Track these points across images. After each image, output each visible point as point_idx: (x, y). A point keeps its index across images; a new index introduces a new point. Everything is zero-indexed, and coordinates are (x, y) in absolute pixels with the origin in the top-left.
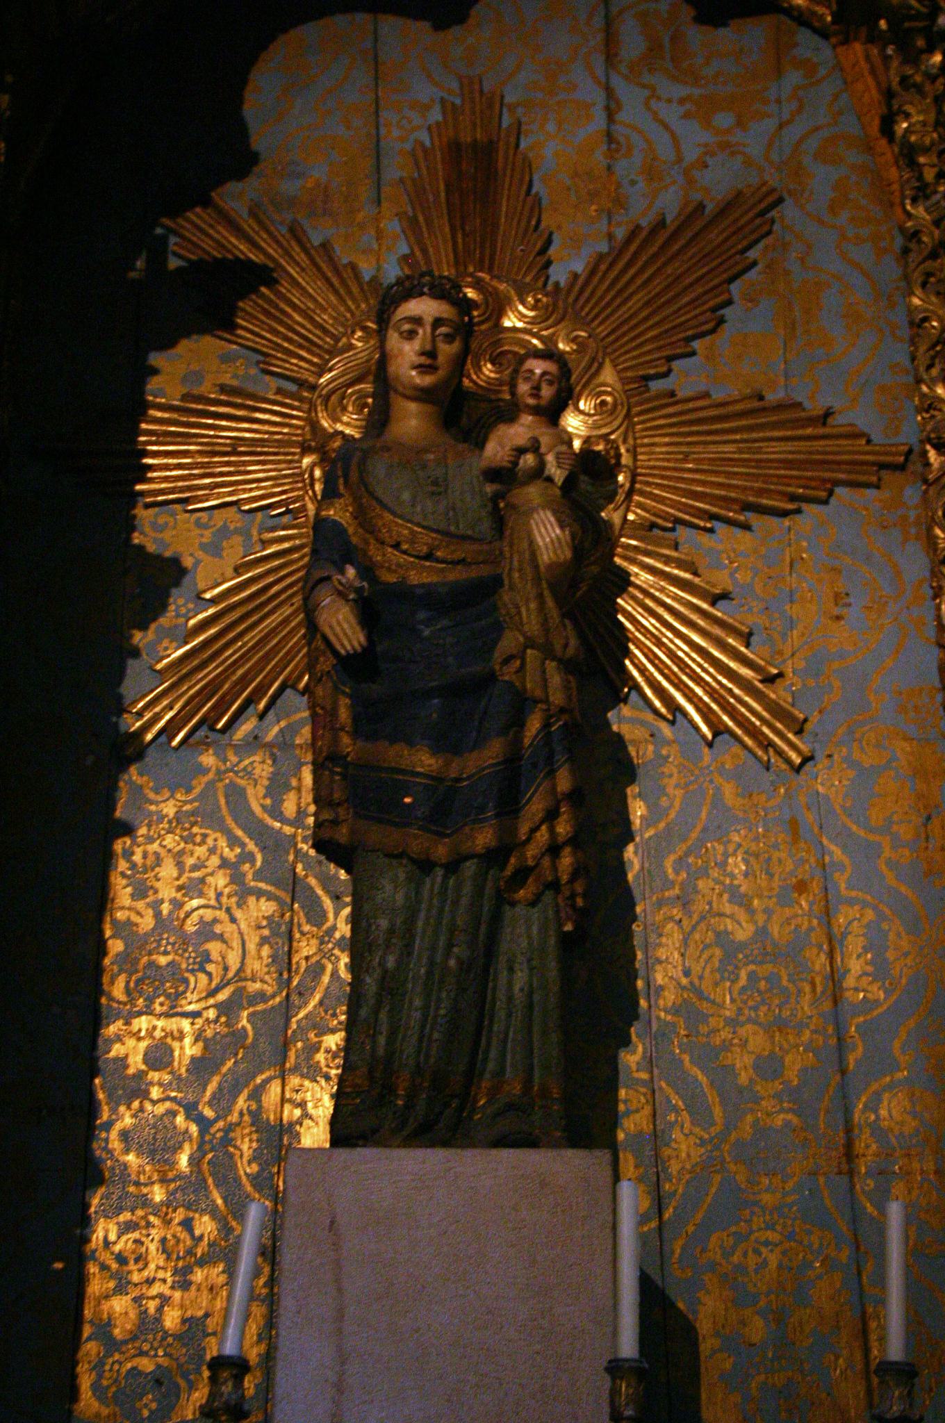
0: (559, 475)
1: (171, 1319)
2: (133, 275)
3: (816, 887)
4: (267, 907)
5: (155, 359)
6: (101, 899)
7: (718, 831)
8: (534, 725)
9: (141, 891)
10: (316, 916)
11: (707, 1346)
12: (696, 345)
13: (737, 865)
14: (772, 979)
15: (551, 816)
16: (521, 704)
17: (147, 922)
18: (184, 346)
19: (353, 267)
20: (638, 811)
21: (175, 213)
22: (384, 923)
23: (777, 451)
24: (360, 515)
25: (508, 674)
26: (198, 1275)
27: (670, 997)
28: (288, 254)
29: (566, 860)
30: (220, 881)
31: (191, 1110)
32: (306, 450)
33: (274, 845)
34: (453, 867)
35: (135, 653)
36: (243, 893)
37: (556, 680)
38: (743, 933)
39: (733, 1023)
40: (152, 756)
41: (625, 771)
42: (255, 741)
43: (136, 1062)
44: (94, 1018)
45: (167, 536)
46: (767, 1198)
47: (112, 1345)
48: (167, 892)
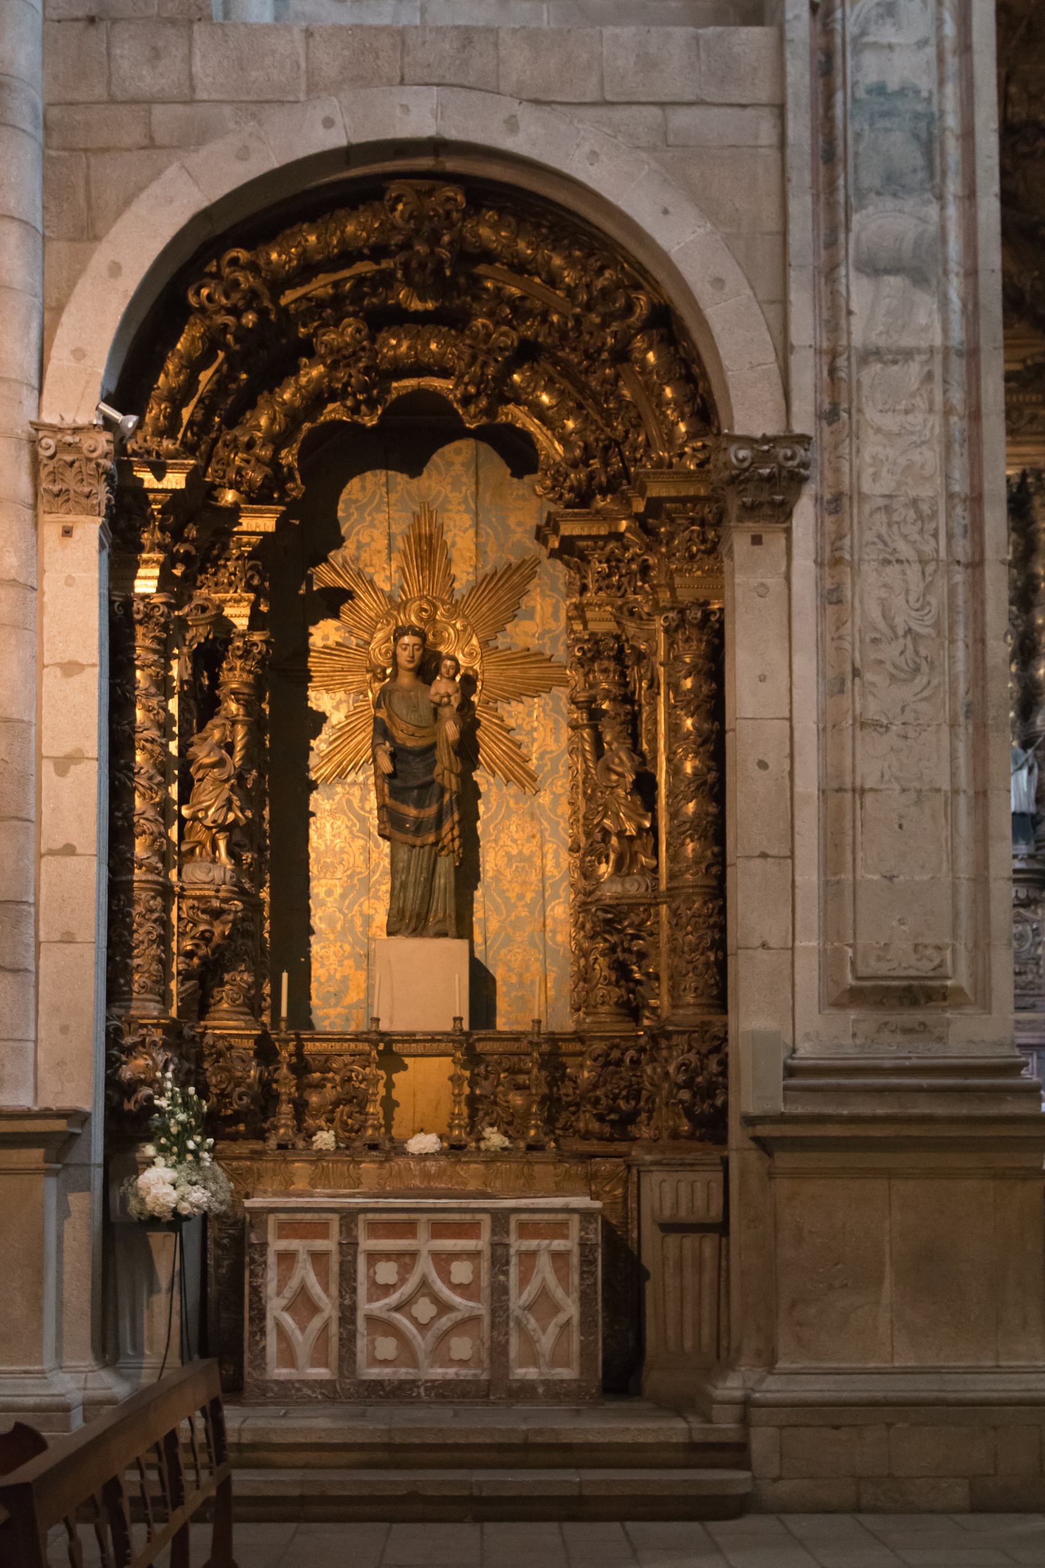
0: (456, 705)
1: (338, 976)
2: (301, 592)
3: (538, 836)
4: (361, 842)
5: (312, 630)
6: (306, 839)
7: (508, 816)
8: (447, 797)
9: (320, 837)
10: (378, 846)
11: (499, 984)
12: (508, 626)
13: (513, 828)
14: (523, 868)
15: (452, 829)
16: (442, 791)
17: (323, 848)
18: (322, 623)
19: (382, 591)
20: (481, 809)
21: (314, 565)
22: (401, 865)
23: (534, 673)
24: (389, 716)
25: (439, 779)
26: (346, 962)
27: (490, 874)
28: (357, 585)
29: (457, 843)
30: (346, 832)
31: (340, 911)
32: (368, 671)
33: (363, 820)
34: (422, 847)
35: (312, 749)
36: (354, 837)
37: (454, 780)
38: (514, 852)
39: (510, 882)
40: (321, 788)
41: (478, 795)
42: (354, 783)
43: (322, 895)
44: (308, 880)
45: (320, 703)
46: (519, 939)
47: (321, 984)
48: (328, 837)
